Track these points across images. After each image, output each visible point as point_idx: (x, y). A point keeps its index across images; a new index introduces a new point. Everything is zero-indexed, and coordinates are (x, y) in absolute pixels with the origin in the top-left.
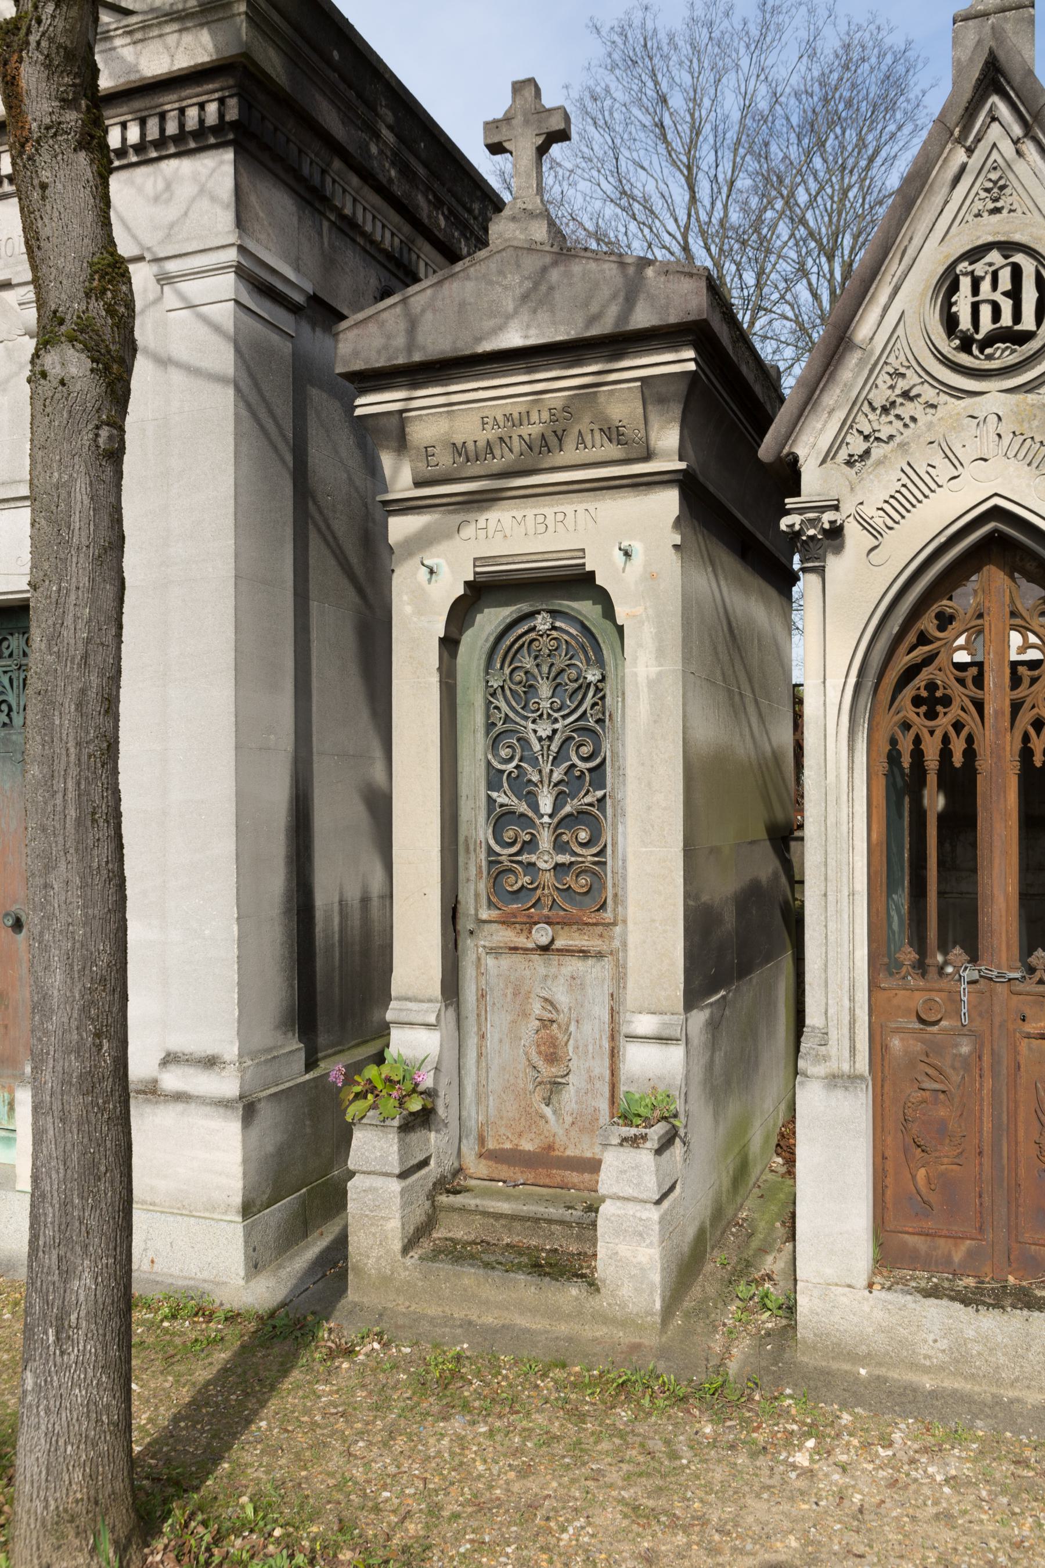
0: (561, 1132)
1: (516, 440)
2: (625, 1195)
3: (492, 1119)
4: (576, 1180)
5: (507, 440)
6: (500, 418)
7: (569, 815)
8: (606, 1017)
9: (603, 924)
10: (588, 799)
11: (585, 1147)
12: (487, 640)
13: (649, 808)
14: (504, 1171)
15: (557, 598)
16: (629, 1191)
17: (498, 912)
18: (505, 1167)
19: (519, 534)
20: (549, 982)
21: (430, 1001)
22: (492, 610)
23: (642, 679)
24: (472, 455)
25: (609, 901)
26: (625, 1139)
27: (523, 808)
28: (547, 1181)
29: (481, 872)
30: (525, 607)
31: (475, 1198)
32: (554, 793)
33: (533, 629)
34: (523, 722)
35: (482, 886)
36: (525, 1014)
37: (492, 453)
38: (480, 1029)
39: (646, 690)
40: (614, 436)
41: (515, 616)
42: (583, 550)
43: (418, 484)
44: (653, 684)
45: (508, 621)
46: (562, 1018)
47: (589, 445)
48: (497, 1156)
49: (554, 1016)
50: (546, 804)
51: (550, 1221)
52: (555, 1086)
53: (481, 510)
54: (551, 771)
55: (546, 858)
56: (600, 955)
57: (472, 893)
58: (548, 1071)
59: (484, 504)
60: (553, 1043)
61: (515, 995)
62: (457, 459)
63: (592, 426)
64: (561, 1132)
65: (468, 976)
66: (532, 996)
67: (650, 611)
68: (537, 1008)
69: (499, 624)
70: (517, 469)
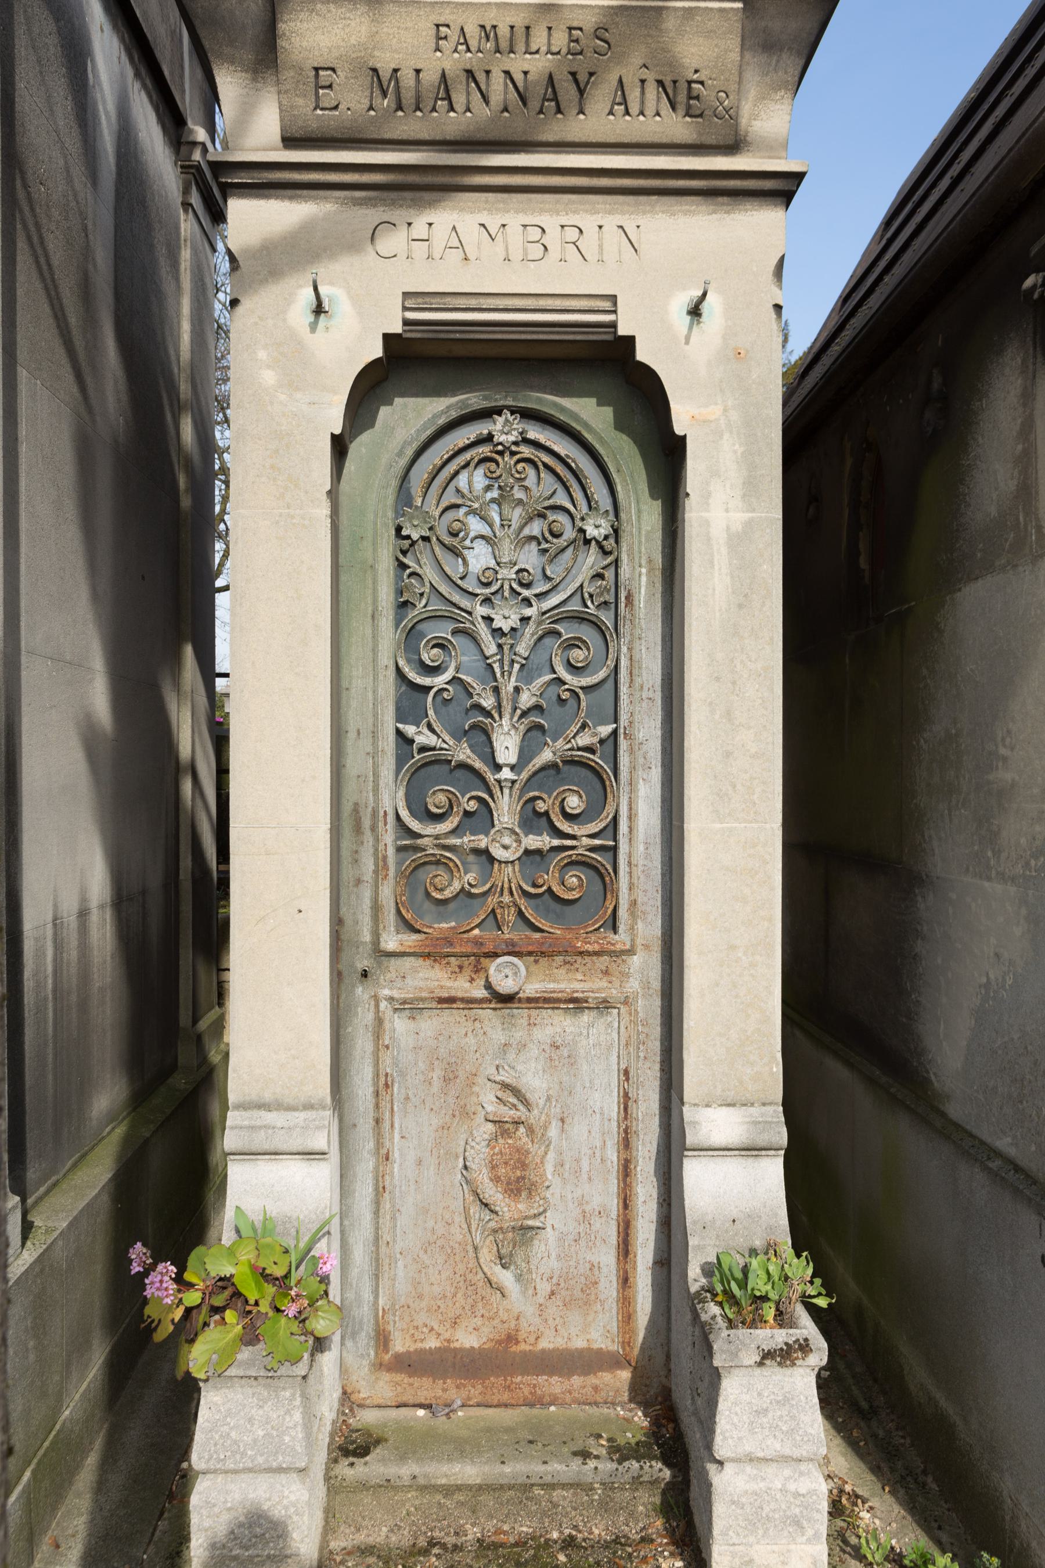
0: (529, 1310)
1: (498, 80)
2: (768, 1454)
3: (403, 1301)
4: (557, 1390)
5: (481, 77)
6: (472, 32)
7: (551, 767)
8: (613, 1109)
9: (612, 954)
10: (584, 740)
11: (574, 1331)
12: (400, 454)
13: (728, 754)
14: (426, 1389)
15: (532, 388)
16: (775, 1446)
17: (415, 937)
18: (427, 1382)
19: (497, 255)
20: (511, 1056)
21: (309, 1107)
22: (411, 401)
23: (718, 532)
24: (408, 97)
25: (623, 913)
26: (767, 1356)
27: (464, 753)
28: (506, 1397)
29: (386, 867)
30: (475, 400)
31: (403, 1458)
32: (522, 728)
33: (489, 438)
34: (465, 603)
35: (387, 892)
36: (465, 1113)
37: (448, 98)
38: (379, 1145)
39: (724, 550)
40: (682, 97)
41: (454, 414)
42: (613, 298)
43: (289, 141)
44: (737, 540)
45: (442, 421)
46: (534, 1117)
47: (634, 109)
48: (409, 1364)
49: (522, 1113)
50: (507, 745)
51: (551, 1487)
52: (525, 1232)
53: (421, 205)
54: (517, 690)
55: (507, 840)
56: (604, 1006)
57: (367, 903)
58: (510, 1210)
59: (427, 196)
60: (521, 1160)
61: (446, 1080)
62: (378, 101)
63: (645, 74)
64: (529, 1310)
65: (357, 1053)
66: (481, 1080)
67: (734, 416)
68: (488, 1099)
69: (424, 427)
70: (491, 136)
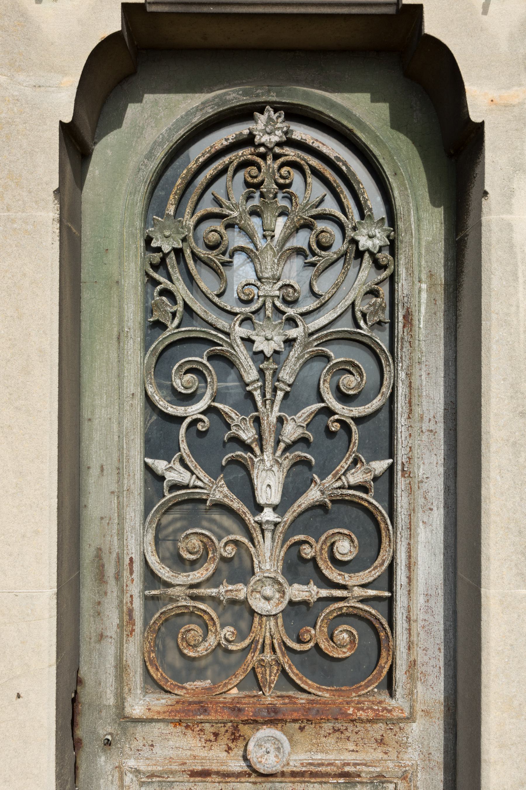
9: (386, 721)
10: (356, 477)
12: (150, 156)
15: (298, 82)
22: (162, 98)
25: (400, 675)
27: (220, 492)
30: (234, 96)
32: (286, 464)
34: (222, 323)
35: (133, 650)
41: (210, 111)
45: (196, 119)
50: (269, 484)
54: (281, 420)
55: (268, 591)
69: (177, 126)
